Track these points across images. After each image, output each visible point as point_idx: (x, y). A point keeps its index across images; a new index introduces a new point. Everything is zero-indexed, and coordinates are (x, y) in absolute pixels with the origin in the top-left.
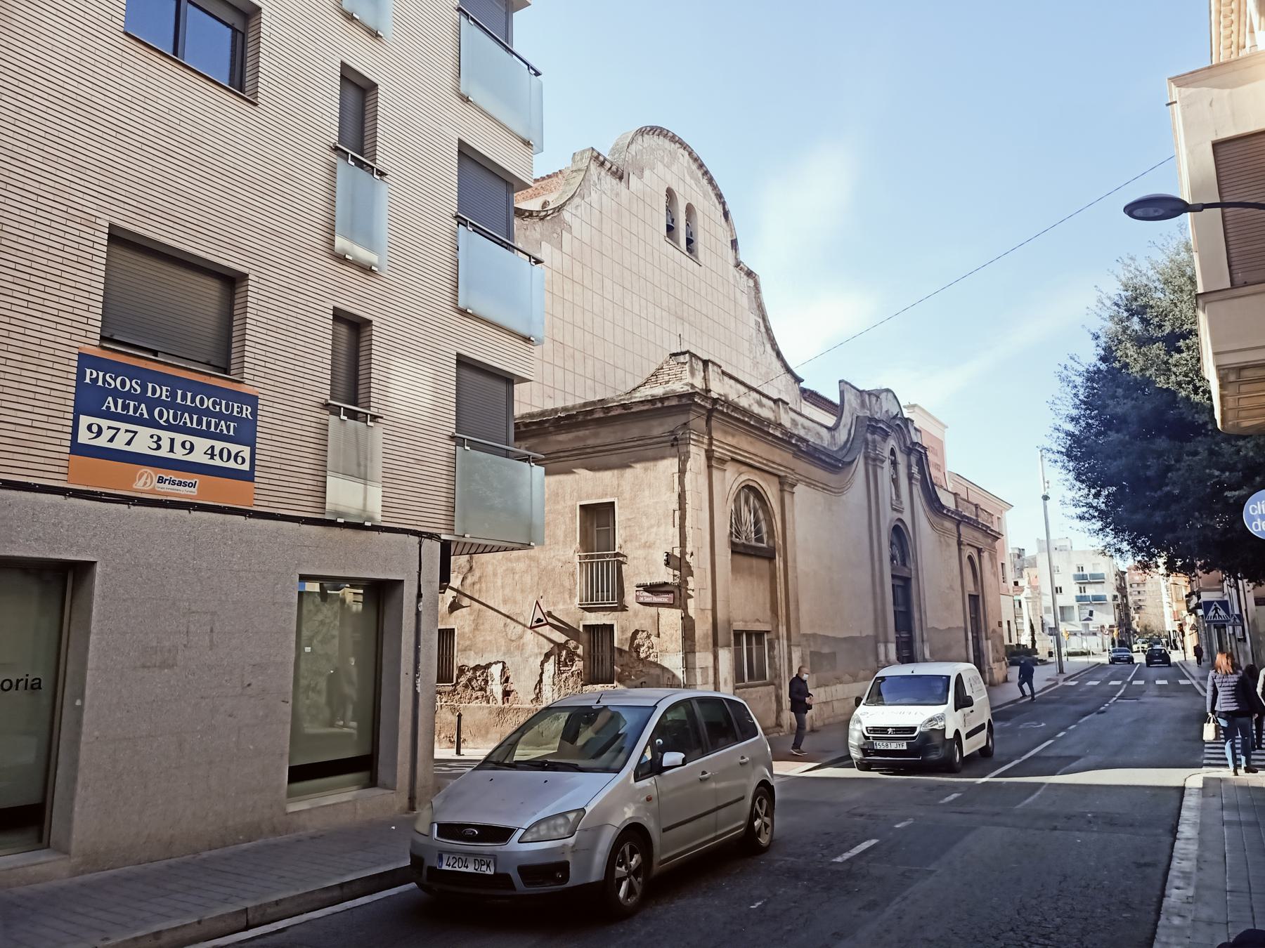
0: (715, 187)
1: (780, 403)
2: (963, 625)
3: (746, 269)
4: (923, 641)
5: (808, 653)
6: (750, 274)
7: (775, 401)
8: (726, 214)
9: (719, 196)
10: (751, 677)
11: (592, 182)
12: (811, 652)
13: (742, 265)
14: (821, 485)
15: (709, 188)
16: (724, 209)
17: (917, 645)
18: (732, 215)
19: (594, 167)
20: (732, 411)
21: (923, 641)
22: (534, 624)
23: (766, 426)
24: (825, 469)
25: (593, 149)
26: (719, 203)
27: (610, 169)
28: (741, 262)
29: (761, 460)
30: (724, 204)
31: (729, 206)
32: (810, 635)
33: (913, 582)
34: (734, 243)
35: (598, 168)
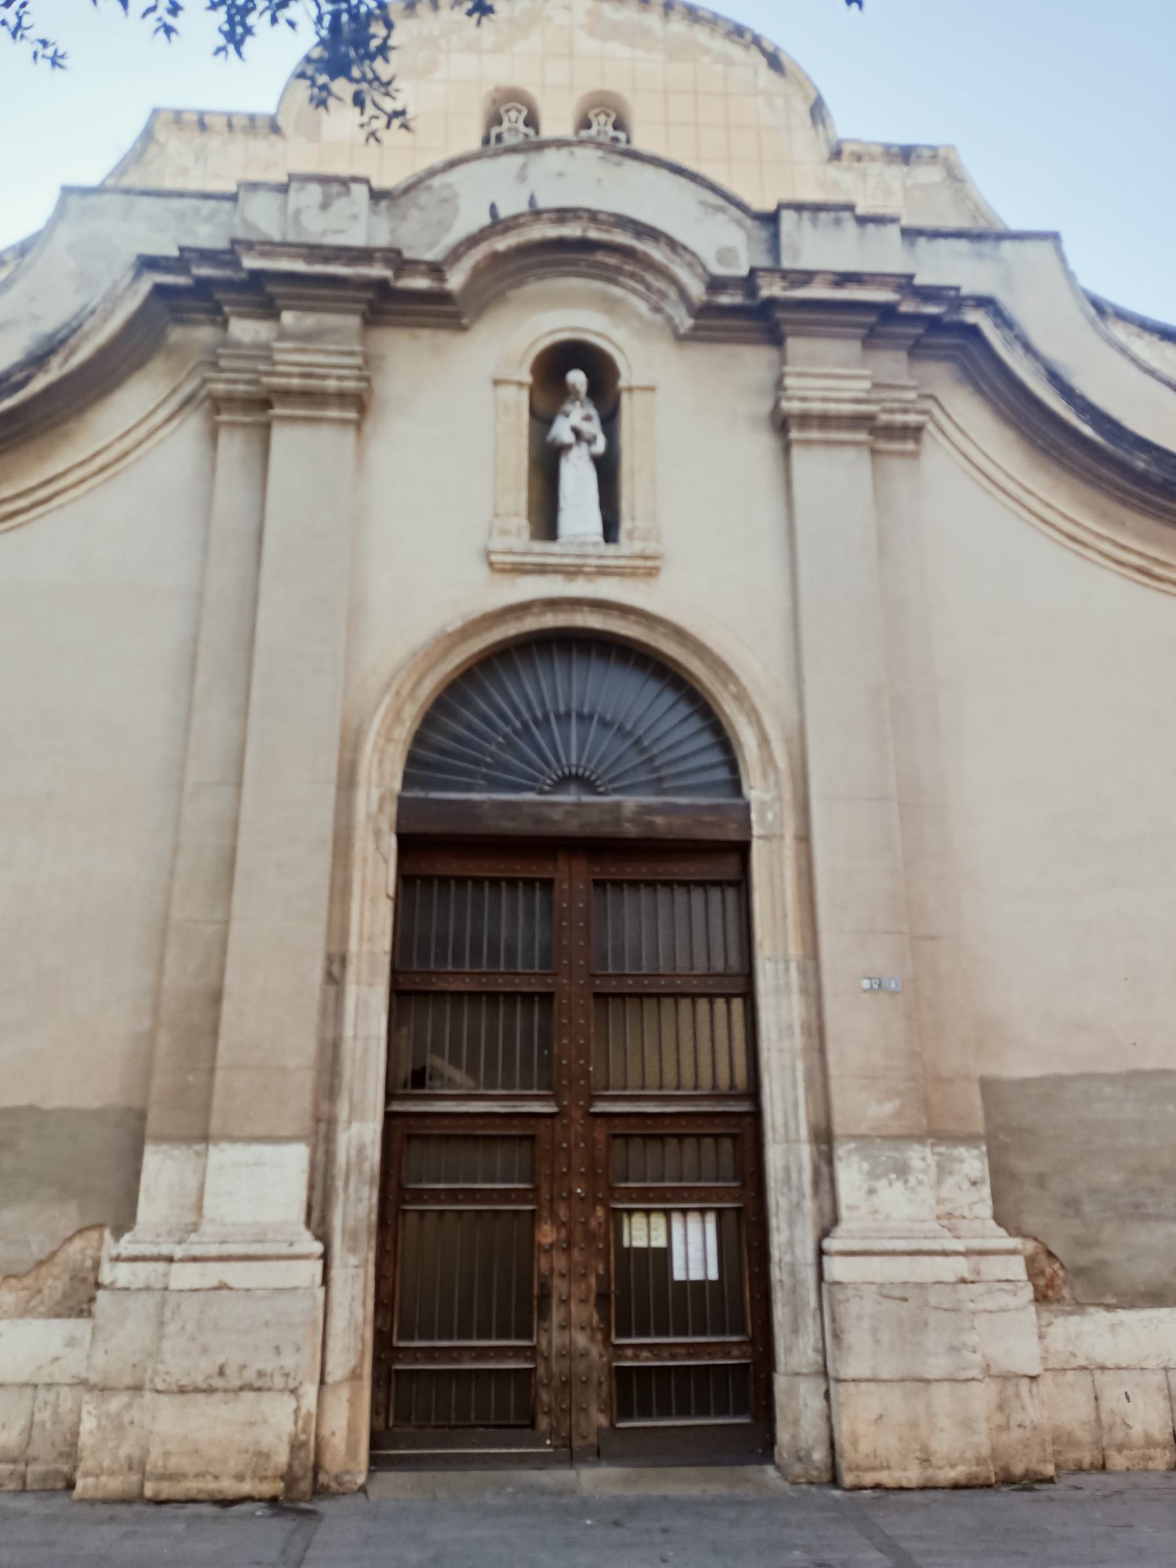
0: (713, 21)
3: (877, 150)
6: (906, 155)
8: (774, 61)
9: (737, 32)
13: (847, 149)
15: (701, 34)
16: (763, 51)
18: (792, 50)
26: (746, 47)
27: (230, 126)
28: (840, 142)
30: (757, 41)
31: (772, 37)
34: (817, 111)
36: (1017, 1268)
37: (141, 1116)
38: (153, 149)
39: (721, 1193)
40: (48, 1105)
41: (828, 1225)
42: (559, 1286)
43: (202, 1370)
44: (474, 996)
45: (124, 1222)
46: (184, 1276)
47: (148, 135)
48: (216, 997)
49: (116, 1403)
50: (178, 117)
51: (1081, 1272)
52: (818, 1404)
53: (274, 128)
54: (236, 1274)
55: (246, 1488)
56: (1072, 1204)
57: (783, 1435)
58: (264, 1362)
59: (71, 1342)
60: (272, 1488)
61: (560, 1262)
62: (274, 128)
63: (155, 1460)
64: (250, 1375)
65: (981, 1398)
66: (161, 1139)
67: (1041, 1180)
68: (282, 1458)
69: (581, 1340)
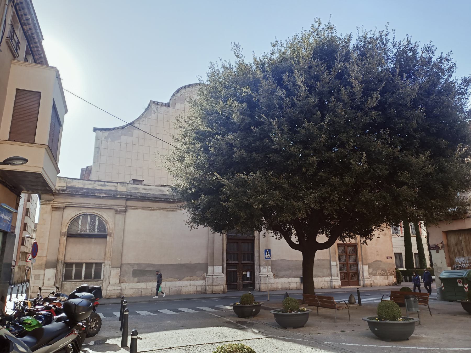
1: (119, 184)
2: (329, 258)
4: (260, 265)
5: (132, 270)
7: (117, 183)
10: (86, 278)
11: (152, 111)
12: (134, 270)
14: (157, 209)
17: (256, 267)
19: (153, 106)
20: (63, 192)
21: (260, 265)
22: (28, 260)
23: (91, 194)
24: (159, 202)
25: (151, 101)
27: (162, 105)
29: (94, 205)
32: (134, 264)
33: (256, 242)
35: (157, 106)
36: (272, 275)
37: (208, 264)
38: (150, 107)
39: (251, 270)
40: (200, 263)
41: (260, 272)
42: (239, 278)
43: (216, 284)
44: (232, 253)
45: (207, 272)
46: (214, 277)
47: (149, 105)
48: (213, 253)
49: (210, 287)
50: (154, 102)
51: (276, 275)
52: (258, 286)
53: (169, 106)
54: (218, 276)
55: (220, 292)
56: (276, 270)
57: (255, 288)
58: (221, 283)
59: (204, 282)
60: (222, 292)
61: (239, 276)
62: (169, 106)
63: (214, 290)
64: (220, 284)
65: (270, 285)
66: (210, 266)
67: (274, 268)
68: (223, 290)
69: (241, 282)
